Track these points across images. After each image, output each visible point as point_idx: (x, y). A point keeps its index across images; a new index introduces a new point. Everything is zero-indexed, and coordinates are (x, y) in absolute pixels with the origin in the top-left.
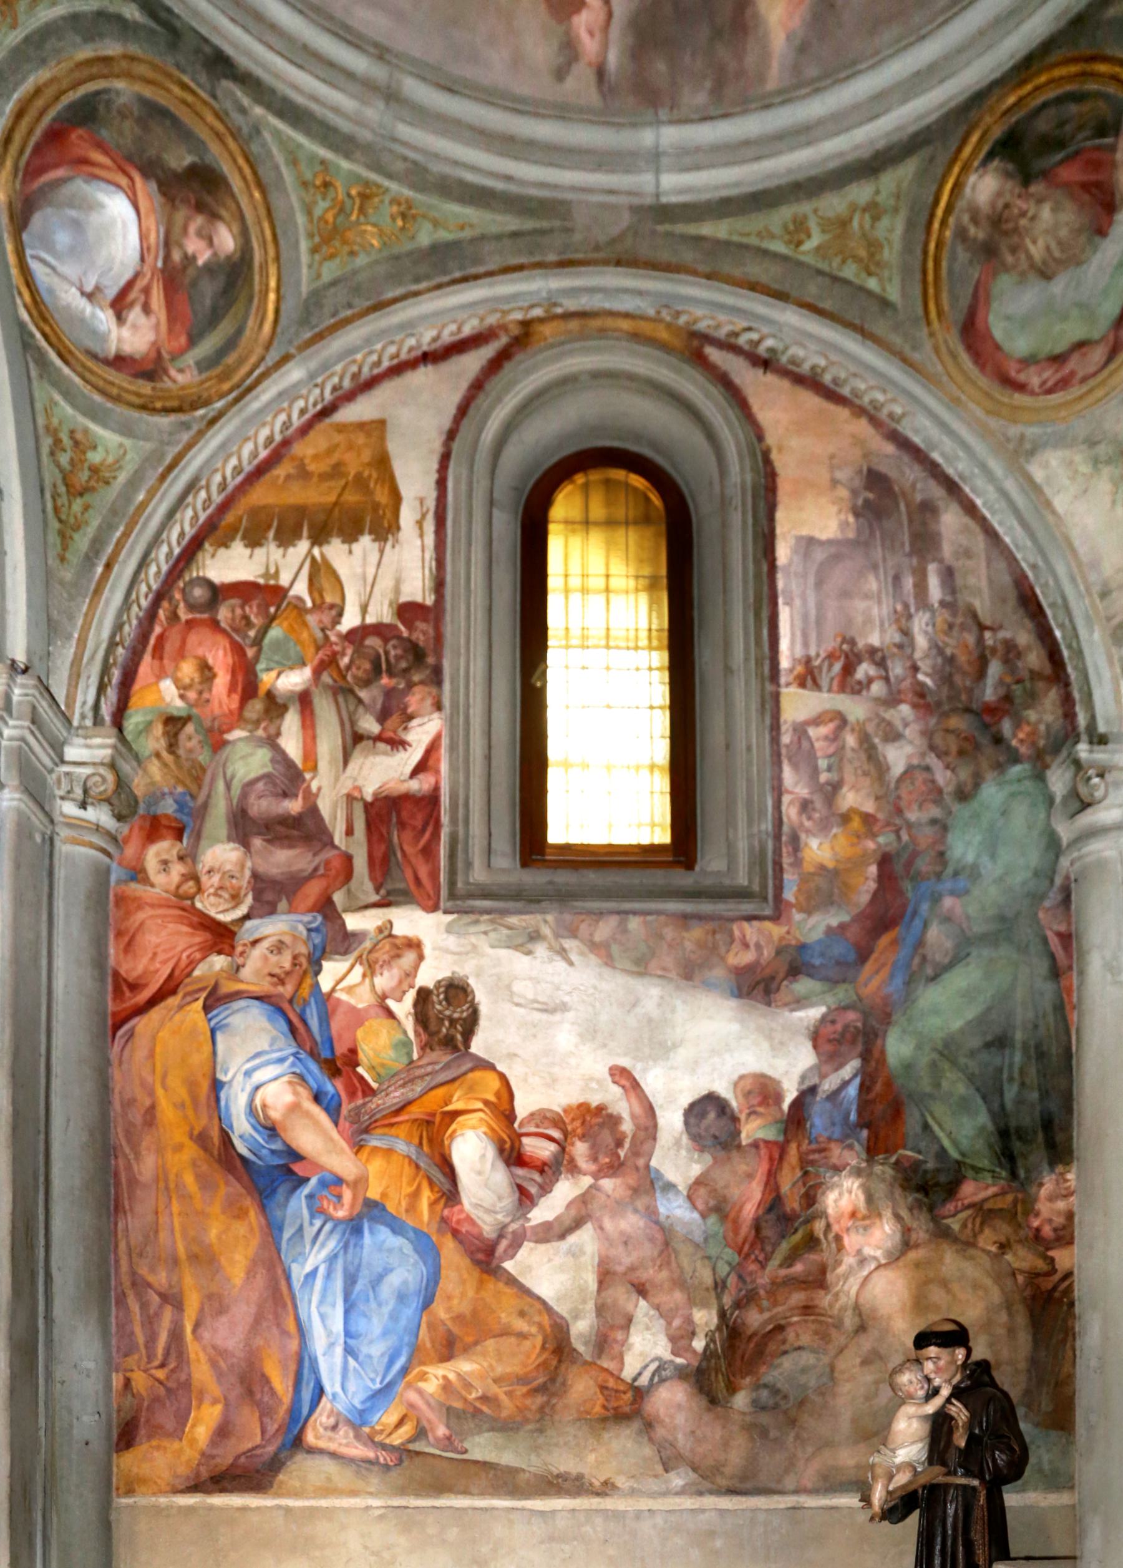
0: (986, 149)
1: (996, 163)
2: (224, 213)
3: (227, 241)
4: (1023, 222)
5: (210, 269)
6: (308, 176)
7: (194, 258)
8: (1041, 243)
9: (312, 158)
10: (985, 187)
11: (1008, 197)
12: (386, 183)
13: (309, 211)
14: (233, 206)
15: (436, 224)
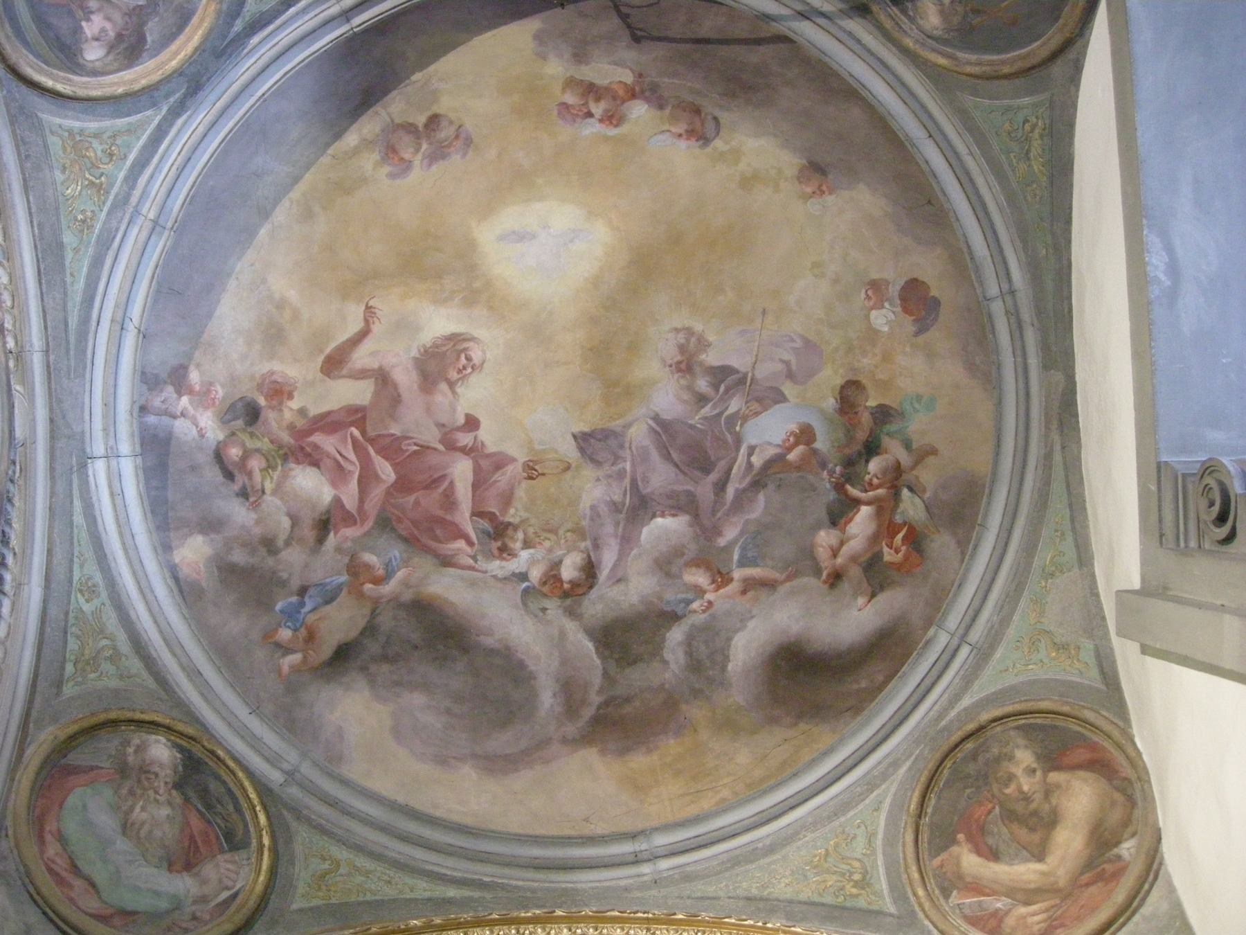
0: (184, 744)
1: (179, 755)
2: (110, 57)
3: (93, 54)
4: (151, 793)
5: (78, 30)
6: (119, 142)
7: (88, 20)
8: (144, 816)
9: (129, 147)
10: (160, 751)
11: (162, 774)
12: (106, 209)
13: (97, 135)
14: (112, 68)
15: (76, 250)
